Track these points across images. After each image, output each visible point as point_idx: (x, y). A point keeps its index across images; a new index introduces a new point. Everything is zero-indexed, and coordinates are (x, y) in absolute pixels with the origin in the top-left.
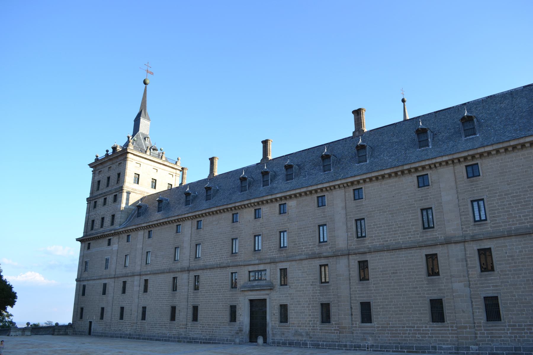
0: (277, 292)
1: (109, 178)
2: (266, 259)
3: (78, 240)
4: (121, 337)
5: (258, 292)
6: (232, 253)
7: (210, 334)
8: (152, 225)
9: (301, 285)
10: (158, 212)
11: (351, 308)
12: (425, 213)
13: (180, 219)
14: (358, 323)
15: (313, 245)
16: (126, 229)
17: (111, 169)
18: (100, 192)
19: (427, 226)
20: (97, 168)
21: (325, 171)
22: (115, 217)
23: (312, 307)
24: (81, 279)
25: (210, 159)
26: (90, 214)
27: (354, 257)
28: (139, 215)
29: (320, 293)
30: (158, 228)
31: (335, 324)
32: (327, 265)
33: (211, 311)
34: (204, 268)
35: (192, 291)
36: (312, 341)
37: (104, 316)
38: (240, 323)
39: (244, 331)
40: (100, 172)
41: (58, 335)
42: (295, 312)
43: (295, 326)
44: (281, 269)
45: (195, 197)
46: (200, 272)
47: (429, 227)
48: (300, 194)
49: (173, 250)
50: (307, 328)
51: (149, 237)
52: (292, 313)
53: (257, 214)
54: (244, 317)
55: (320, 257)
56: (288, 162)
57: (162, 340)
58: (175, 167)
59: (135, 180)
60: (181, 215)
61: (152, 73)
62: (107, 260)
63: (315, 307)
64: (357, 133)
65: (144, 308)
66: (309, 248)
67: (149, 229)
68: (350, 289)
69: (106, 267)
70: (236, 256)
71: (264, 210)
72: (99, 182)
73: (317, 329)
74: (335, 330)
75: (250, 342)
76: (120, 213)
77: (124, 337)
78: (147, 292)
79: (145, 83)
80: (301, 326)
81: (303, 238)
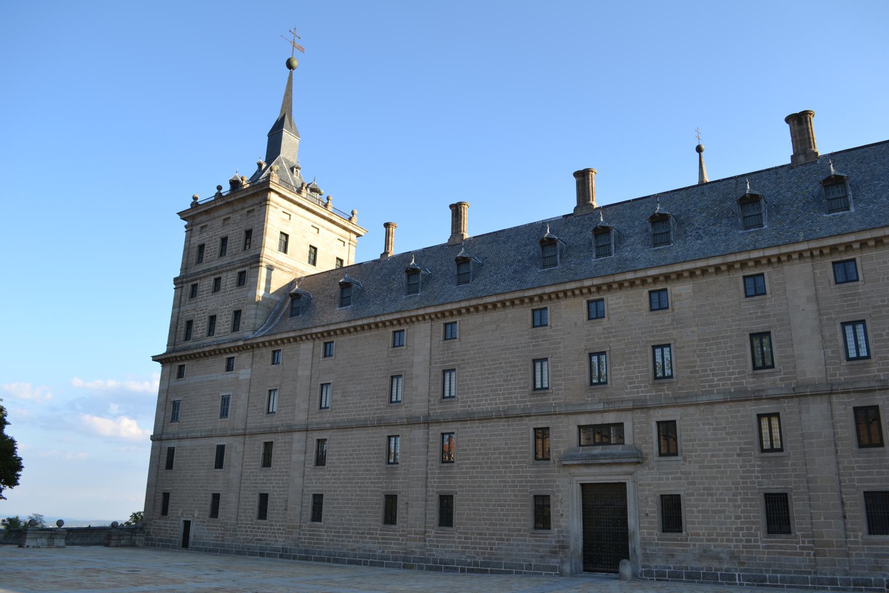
0: (653, 468)
1: (224, 240)
2: (622, 401)
3: (155, 359)
4: (262, 555)
5: (605, 469)
6: (535, 389)
7: (484, 553)
8: (335, 331)
9: (713, 456)
10: (341, 306)
11: (843, 503)
12: (756, 342)
13: (405, 318)
14: (860, 534)
15: (739, 373)
16: (273, 338)
17: (231, 221)
18: (204, 266)
19: (762, 362)
20: (198, 220)
21: (747, 228)
22: (243, 316)
23: (742, 500)
24: (164, 437)
25: (451, 206)
26: (182, 309)
27: (845, 398)
28: (294, 312)
29: (759, 472)
30: (347, 337)
31: (803, 536)
32: (777, 415)
33: (486, 505)
34: (468, 418)
35: (438, 464)
36: (746, 570)
37: (220, 511)
38: (559, 532)
39: (572, 548)
40: (202, 227)
41: (117, 546)
42: (699, 511)
43: (701, 540)
44: (658, 423)
45: (428, 278)
46: (458, 425)
47: (764, 367)
48: (704, 271)
49: (387, 381)
50: (732, 544)
51: (327, 354)
52: (692, 512)
53: (397, 339)
54: (569, 520)
55: (759, 399)
56: (461, 253)
57: (365, 564)
58: (350, 227)
59: (280, 245)
60: (409, 311)
61: (302, 50)
62: (225, 400)
63: (751, 500)
64: (802, 159)
65: (318, 499)
66: (730, 379)
67: (327, 342)
68: (838, 463)
69: (224, 414)
70: (545, 394)
71: (610, 302)
72: (201, 247)
73: (758, 547)
74: (801, 548)
75: (585, 570)
76: (254, 306)
77: (269, 555)
78: (324, 464)
79: (289, 65)
80: (716, 540)
81: (712, 360)
